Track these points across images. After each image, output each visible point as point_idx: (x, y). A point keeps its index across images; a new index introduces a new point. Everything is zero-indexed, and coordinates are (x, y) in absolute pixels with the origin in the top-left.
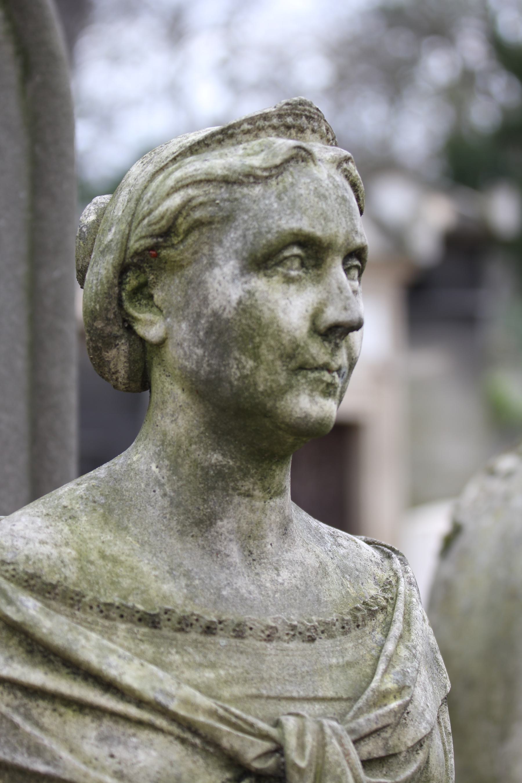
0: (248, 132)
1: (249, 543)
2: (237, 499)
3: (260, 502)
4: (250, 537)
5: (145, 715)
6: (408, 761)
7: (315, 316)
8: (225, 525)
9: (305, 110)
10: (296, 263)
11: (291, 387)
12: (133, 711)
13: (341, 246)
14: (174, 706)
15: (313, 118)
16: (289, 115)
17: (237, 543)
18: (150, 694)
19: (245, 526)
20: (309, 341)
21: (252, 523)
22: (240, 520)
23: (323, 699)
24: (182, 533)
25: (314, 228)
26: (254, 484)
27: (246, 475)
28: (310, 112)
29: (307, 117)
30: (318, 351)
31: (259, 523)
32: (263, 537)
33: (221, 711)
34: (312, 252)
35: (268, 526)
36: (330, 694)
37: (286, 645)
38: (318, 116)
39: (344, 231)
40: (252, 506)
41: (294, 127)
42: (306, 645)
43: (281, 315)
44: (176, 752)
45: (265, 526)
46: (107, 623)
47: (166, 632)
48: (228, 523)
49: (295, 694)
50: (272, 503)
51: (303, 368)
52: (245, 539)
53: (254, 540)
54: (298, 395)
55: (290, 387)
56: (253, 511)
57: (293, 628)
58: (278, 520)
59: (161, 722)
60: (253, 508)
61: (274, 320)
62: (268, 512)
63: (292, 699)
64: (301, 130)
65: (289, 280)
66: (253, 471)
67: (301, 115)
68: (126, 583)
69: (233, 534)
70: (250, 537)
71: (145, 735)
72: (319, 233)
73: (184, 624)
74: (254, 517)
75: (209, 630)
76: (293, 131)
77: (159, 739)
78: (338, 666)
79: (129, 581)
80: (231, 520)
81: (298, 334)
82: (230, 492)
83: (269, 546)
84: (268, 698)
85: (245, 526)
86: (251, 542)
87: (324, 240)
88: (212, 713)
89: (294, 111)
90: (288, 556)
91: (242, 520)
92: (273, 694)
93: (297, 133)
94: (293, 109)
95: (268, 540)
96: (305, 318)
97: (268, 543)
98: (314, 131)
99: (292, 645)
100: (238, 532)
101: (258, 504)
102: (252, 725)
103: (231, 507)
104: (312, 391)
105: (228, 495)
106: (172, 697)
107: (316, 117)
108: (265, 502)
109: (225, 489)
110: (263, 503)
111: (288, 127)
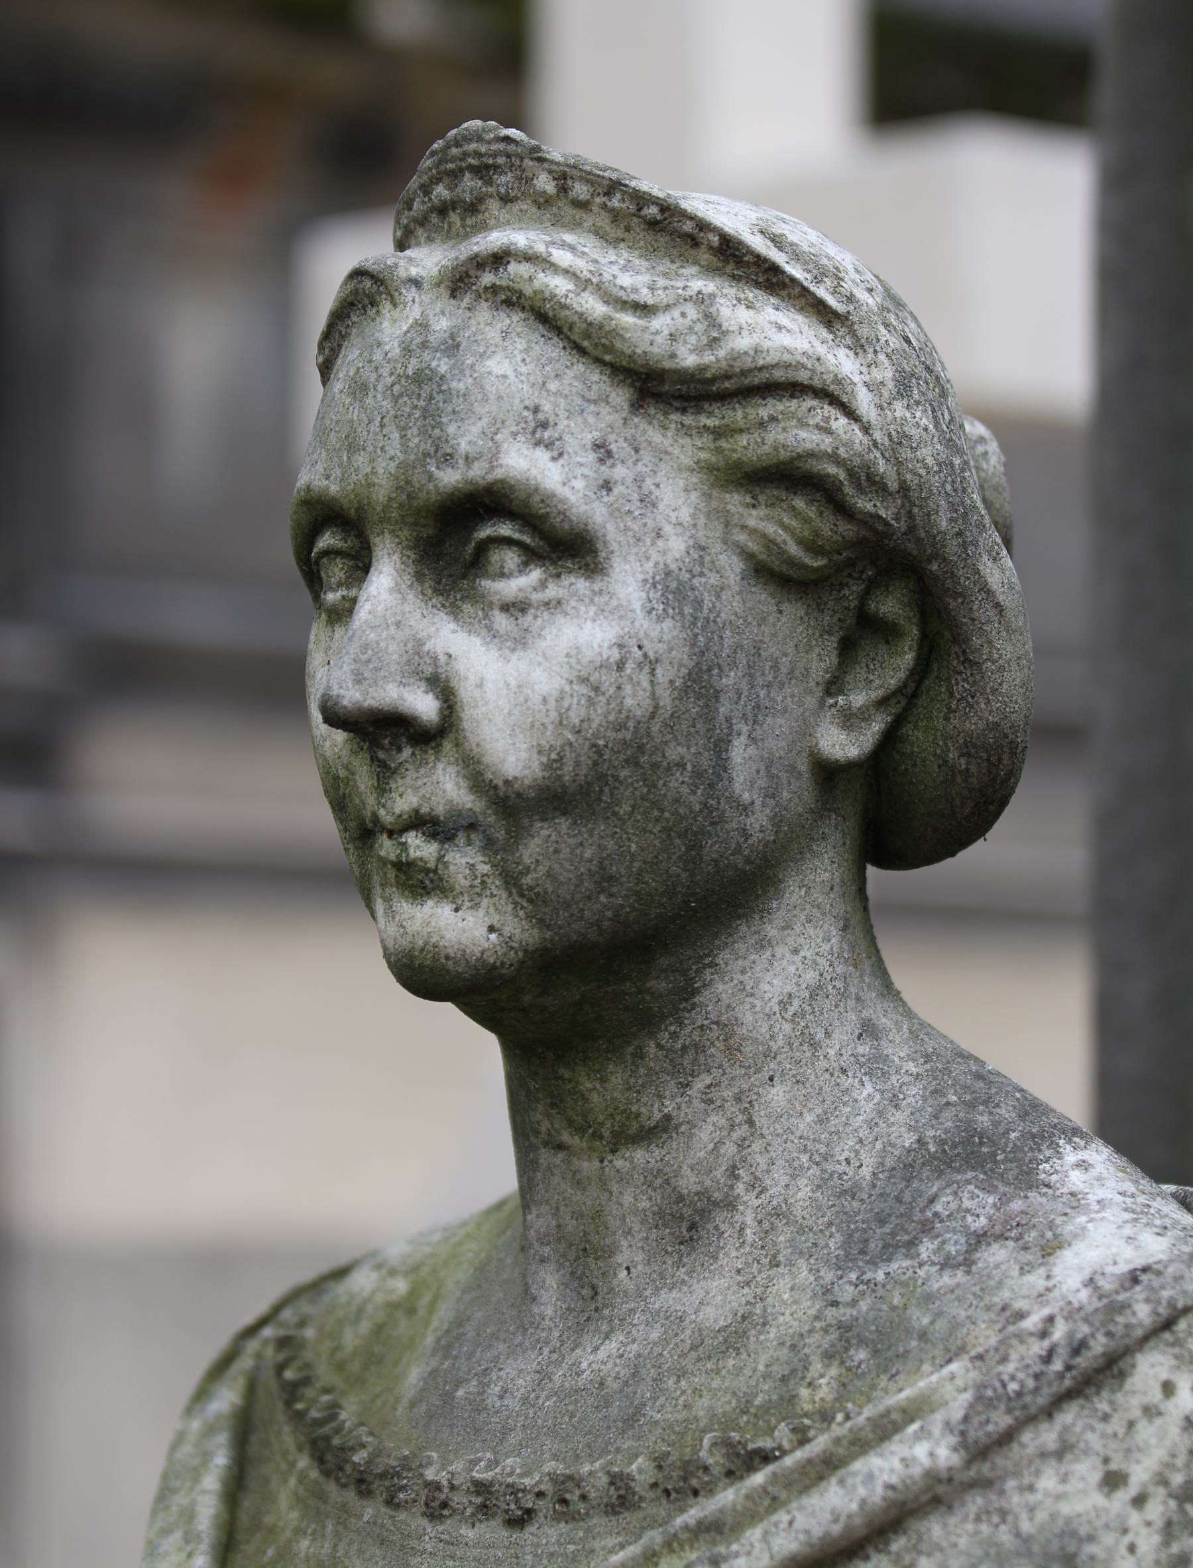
1: (586, 1266)
3: (590, 1160)
4: (585, 1250)
9: (465, 155)
13: (386, 507)
15: (496, 167)
17: (561, 1266)
19: (571, 1225)
21: (582, 1215)
22: (557, 1208)
28: (478, 154)
29: (473, 169)
31: (598, 1215)
35: (618, 1223)
38: (508, 156)
39: (392, 466)
40: (574, 1173)
45: (614, 1224)
48: (538, 1216)
50: (619, 1163)
52: (577, 1259)
56: (580, 1184)
58: (644, 1204)
60: (578, 1176)
62: (615, 1188)
64: (473, 208)
67: (462, 170)
69: (548, 1243)
70: (585, 1250)
72: (334, 489)
76: (454, 217)
83: (623, 1274)
85: (571, 1225)
86: (591, 1260)
87: (345, 503)
89: (442, 168)
91: (562, 1208)
93: (463, 219)
94: (440, 162)
95: (619, 1259)
97: (620, 1265)
98: (506, 200)
100: (559, 1240)
101: (588, 1166)
103: (539, 1175)
107: (501, 160)
108: (602, 1161)
110: (597, 1163)
111: (443, 210)
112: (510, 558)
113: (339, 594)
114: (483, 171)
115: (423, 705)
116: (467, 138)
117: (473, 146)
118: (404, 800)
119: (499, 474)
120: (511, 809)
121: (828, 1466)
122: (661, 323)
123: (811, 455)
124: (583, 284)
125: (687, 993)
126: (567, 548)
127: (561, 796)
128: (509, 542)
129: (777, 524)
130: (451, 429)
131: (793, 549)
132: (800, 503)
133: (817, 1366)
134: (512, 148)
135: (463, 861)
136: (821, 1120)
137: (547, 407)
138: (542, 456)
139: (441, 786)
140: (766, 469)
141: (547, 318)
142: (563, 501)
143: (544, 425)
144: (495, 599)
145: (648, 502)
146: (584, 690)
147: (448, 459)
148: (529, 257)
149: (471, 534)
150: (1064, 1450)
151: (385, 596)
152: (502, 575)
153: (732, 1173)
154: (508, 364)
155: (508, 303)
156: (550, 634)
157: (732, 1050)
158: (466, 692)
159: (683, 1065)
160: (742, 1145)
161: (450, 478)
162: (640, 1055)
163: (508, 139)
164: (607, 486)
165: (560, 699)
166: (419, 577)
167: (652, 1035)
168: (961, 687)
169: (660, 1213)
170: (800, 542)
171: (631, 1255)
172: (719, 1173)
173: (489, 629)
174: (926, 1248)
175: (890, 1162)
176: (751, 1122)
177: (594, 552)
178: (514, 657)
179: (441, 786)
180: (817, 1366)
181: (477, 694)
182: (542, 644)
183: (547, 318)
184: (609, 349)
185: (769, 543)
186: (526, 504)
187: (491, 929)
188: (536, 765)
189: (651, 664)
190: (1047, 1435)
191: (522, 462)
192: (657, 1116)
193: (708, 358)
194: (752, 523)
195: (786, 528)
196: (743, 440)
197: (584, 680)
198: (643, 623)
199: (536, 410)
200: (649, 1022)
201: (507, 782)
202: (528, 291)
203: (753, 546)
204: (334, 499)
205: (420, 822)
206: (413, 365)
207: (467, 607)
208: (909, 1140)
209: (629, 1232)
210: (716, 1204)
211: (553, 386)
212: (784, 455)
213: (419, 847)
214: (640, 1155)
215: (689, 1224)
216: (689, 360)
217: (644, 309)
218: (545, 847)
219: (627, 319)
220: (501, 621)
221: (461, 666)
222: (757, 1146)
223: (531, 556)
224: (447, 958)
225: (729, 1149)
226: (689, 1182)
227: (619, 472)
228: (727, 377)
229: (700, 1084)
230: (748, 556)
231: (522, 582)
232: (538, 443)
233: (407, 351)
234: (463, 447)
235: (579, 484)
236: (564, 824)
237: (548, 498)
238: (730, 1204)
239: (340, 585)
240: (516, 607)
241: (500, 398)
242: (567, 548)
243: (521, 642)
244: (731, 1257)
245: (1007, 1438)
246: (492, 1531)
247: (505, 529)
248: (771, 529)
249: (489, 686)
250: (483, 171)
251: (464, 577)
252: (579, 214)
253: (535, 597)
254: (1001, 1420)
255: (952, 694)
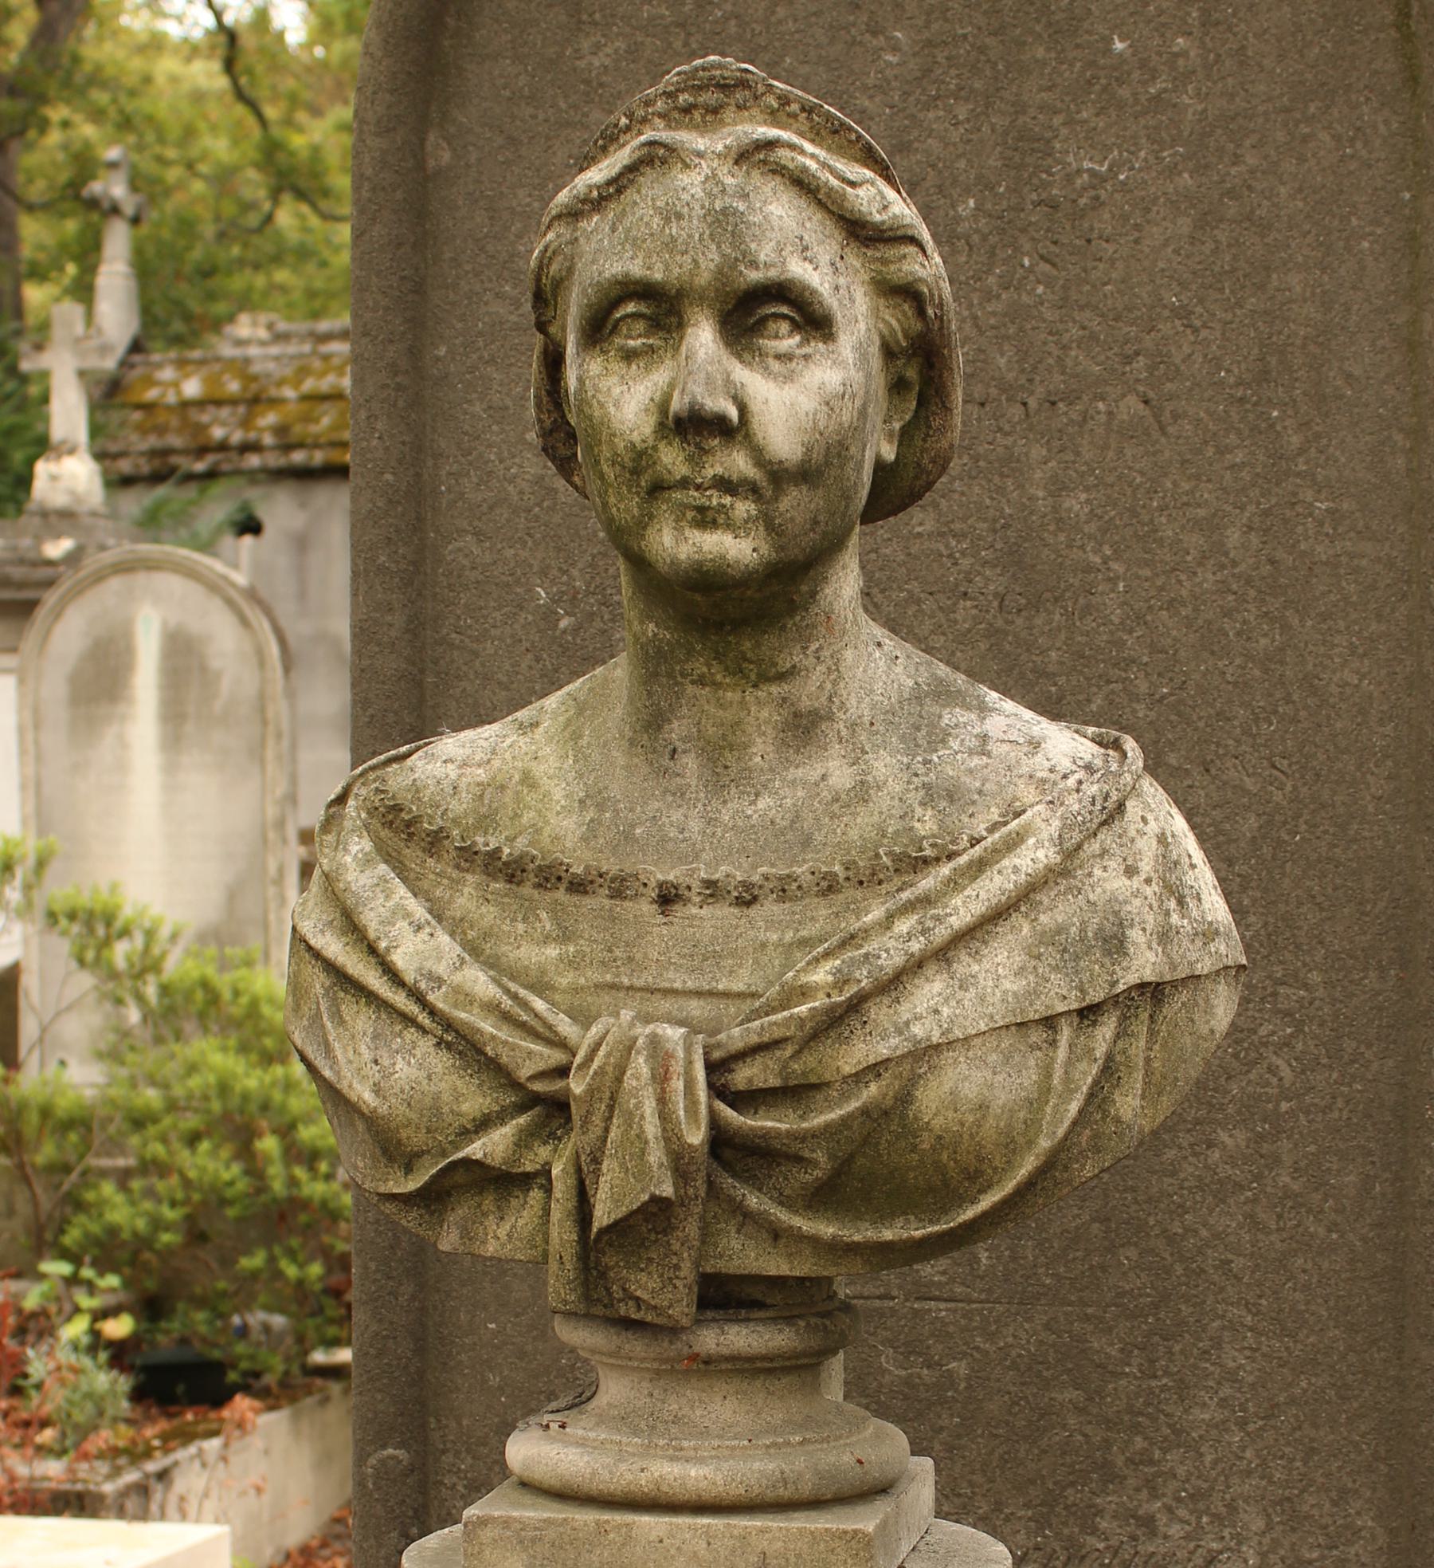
0: (628, 128)
2: (690, 689)
3: (734, 691)
5: (412, 1008)
6: (845, 1097)
7: (663, 407)
8: (676, 730)
10: (640, 326)
11: (651, 517)
12: (400, 1000)
14: (435, 998)
16: (682, 91)
18: (409, 977)
20: (662, 446)
23: (726, 995)
24: (632, 743)
25: (649, 268)
26: (709, 666)
27: (690, 653)
30: (672, 459)
31: (737, 724)
32: (746, 746)
33: (507, 1003)
34: (661, 308)
36: (738, 986)
37: (694, 910)
39: (712, 266)
41: (694, 106)
42: (735, 911)
43: (612, 410)
44: (441, 1061)
46: (455, 874)
47: (527, 890)
49: (678, 985)
51: (658, 488)
53: (731, 750)
54: (660, 530)
55: (645, 521)
57: (709, 884)
59: (424, 1019)
61: (606, 422)
63: (674, 992)
65: (629, 356)
66: (699, 647)
68: (528, 817)
71: (411, 1034)
72: (658, 276)
73: (550, 876)
74: (728, 715)
75: (579, 886)
77: (426, 1045)
78: (779, 944)
79: (532, 814)
80: (685, 721)
81: (636, 437)
82: (679, 679)
84: (631, 988)
88: (492, 1008)
89: (690, 83)
90: (793, 773)
92: (639, 983)
93: (703, 116)
96: (647, 410)
99: (705, 911)
102: (550, 1027)
104: (677, 521)
105: (677, 684)
106: (440, 981)
109: (670, 675)
111: (687, 110)
112: (784, 327)
113: (639, 342)
114: (723, 87)
115: (733, 413)
116: (713, 66)
117: (718, 72)
118: (713, 469)
119: (789, 275)
120: (779, 476)
121: (980, 866)
122: (861, 192)
123: (920, 280)
124: (824, 165)
125: (813, 594)
126: (815, 322)
127: (806, 474)
128: (785, 317)
129: (897, 320)
130: (753, 246)
131: (900, 335)
132: (906, 307)
133: (919, 811)
134: (750, 76)
135: (743, 508)
136: (865, 671)
137: (806, 237)
138: (809, 267)
139: (739, 463)
140: (900, 287)
141: (802, 184)
142: (821, 295)
143: (806, 248)
144: (771, 352)
145: (852, 300)
146: (825, 408)
147: (754, 264)
148: (792, 147)
149: (758, 310)
150: (1104, 852)
151: (710, 344)
152: (777, 337)
153: (830, 699)
154: (779, 213)
155: (774, 172)
156: (807, 374)
157: (830, 630)
158: (755, 407)
159: (805, 638)
160: (835, 683)
161: (754, 276)
162: (783, 628)
163: (746, 71)
164: (837, 288)
165: (815, 414)
166: (721, 333)
167: (792, 617)
168: (936, 423)
169: (786, 723)
170: (903, 330)
171: (761, 749)
172: (823, 699)
173: (766, 369)
174: (955, 745)
175: (906, 695)
176: (838, 670)
177: (831, 326)
178: (786, 387)
179: (739, 463)
180: (919, 811)
181: (764, 407)
182: (804, 381)
183: (802, 184)
184: (841, 207)
185: (892, 331)
186: (802, 295)
187: (754, 550)
188: (799, 454)
189: (854, 396)
190: (1095, 847)
191: (798, 269)
192: (788, 665)
193: (885, 217)
194: (887, 317)
195: (898, 320)
196: (892, 267)
197: (828, 404)
198: (853, 372)
199: (801, 239)
200: (792, 608)
201: (781, 462)
202: (791, 166)
203: (886, 332)
204: (659, 283)
205: (725, 485)
206: (718, 205)
207: (747, 356)
208: (910, 683)
209: (764, 734)
210: (821, 718)
211: (808, 225)
212: (910, 278)
213: (715, 498)
214: (774, 689)
215: (804, 729)
216: (878, 218)
217: (853, 184)
218: (794, 503)
219: (849, 189)
220: (775, 366)
221: (750, 390)
222: (842, 685)
223: (796, 327)
224: (728, 566)
225: (829, 686)
226: (805, 704)
227: (842, 281)
228: (891, 229)
229: (814, 646)
230: (882, 337)
231: (790, 343)
232: (805, 259)
233: (710, 194)
234: (762, 257)
235: (827, 285)
236: (804, 488)
237: (814, 292)
238: (830, 717)
239: (640, 336)
240: (784, 357)
241: (781, 229)
242: (815, 322)
243: (789, 378)
244: (836, 748)
245: (1079, 847)
246: (724, 912)
247: (785, 310)
248: (894, 322)
249: (771, 403)
250: (723, 87)
251: (742, 336)
252: (791, 121)
253: (798, 352)
254: (1077, 837)
255: (930, 427)
